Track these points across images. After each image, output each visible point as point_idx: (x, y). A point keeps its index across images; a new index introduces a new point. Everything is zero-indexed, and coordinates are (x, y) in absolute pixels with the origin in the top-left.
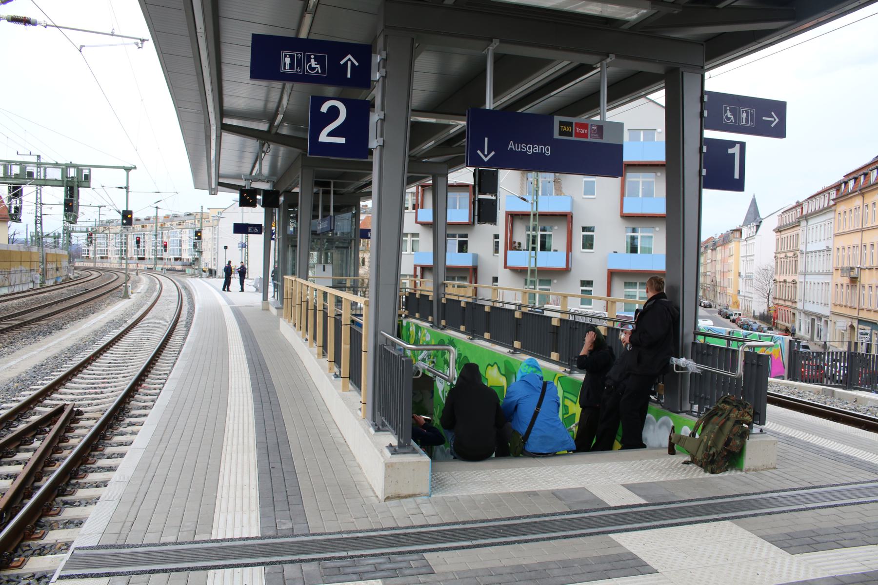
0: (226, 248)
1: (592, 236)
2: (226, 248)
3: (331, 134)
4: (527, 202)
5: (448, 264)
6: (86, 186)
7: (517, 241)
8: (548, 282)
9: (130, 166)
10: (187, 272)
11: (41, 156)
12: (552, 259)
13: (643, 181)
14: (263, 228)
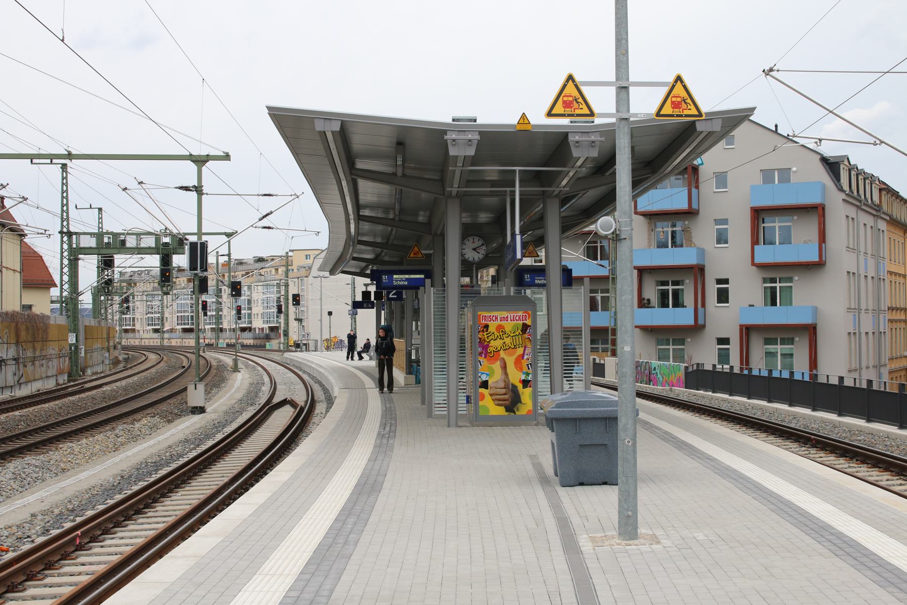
0: (330, 313)
2: (330, 313)
3: (392, 295)
4: (606, 268)
5: (564, 325)
6: (181, 253)
7: (646, 298)
8: (682, 342)
9: (231, 231)
10: (268, 347)
11: (103, 209)
12: (683, 317)
13: (779, 227)
14: (375, 304)
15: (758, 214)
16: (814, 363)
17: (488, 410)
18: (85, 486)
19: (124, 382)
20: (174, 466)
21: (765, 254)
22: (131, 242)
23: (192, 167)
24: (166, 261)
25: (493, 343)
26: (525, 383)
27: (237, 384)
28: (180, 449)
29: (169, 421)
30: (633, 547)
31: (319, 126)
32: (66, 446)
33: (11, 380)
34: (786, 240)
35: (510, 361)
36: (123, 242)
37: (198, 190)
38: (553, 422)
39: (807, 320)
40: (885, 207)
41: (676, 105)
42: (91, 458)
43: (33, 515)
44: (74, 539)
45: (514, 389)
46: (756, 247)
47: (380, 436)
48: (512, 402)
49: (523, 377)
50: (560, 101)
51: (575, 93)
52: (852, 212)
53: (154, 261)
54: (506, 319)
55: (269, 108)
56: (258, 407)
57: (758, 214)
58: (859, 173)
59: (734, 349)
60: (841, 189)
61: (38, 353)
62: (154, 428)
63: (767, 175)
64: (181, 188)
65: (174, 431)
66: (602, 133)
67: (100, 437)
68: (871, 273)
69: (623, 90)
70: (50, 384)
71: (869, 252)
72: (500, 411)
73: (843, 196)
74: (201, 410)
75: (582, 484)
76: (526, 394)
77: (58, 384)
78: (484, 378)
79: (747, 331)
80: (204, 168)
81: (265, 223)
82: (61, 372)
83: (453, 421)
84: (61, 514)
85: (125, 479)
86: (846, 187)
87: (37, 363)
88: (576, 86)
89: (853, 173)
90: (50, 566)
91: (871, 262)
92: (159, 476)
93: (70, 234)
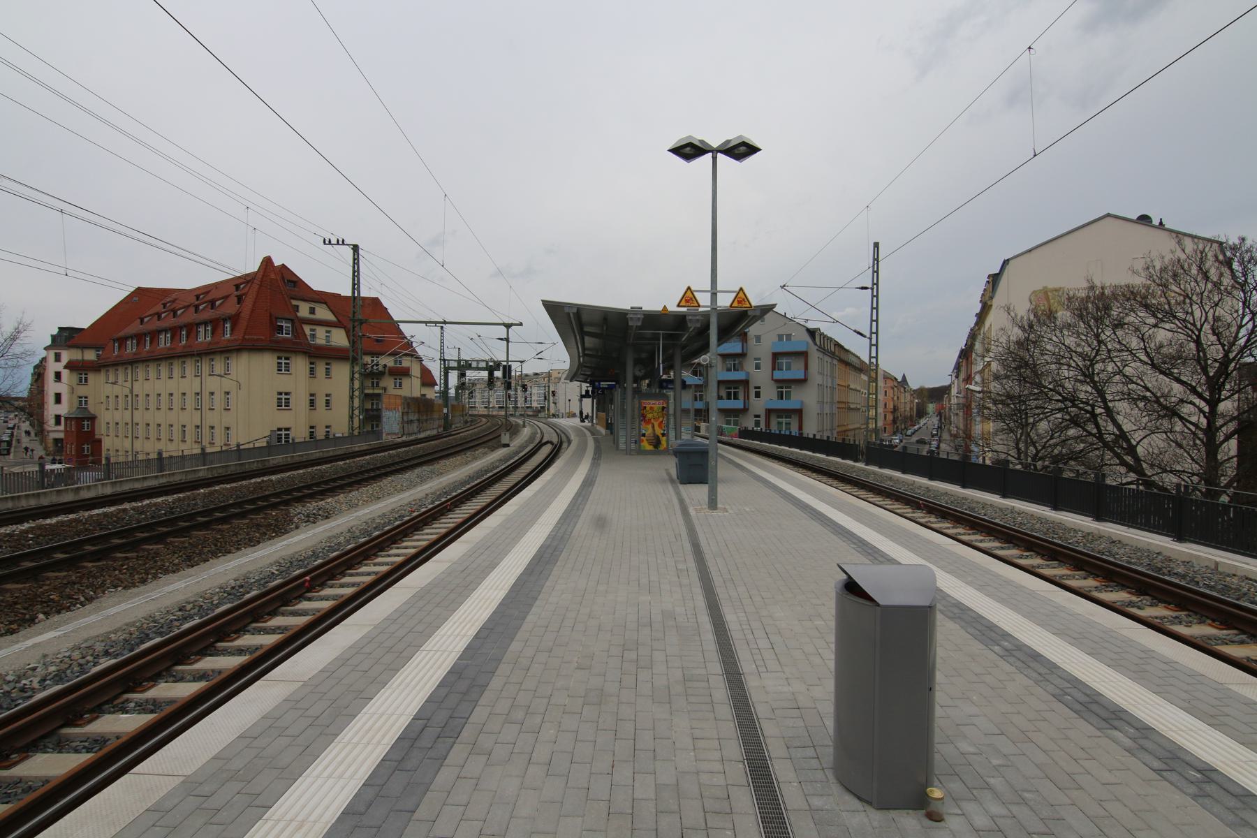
0: (570, 400)
1: (759, 391)
2: (570, 400)
5: (683, 407)
8: (737, 416)
12: (739, 404)
15: (776, 356)
16: (801, 428)
17: (644, 447)
18: (451, 481)
19: (470, 432)
20: (495, 472)
21: (779, 375)
22: (474, 365)
23: (505, 329)
24: (491, 374)
25: (648, 415)
26: (663, 435)
27: (525, 433)
28: (497, 464)
29: (492, 451)
30: (715, 513)
31: (567, 310)
32: (442, 462)
33: (416, 430)
34: (789, 368)
35: (656, 424)
36: (470, 365)
37: (507, 340)
38: (677, 453)
39: (798, 407)
40: (837, 353)
41: (739, 302)
42: (455, 467)
43: (427, 495)
44: (447, 506)
45: (658, 437)
46: (774, 372)
47: (594, 459)
48: (656, 443)
49: (662, 432)
50: (684, 300)
51: (692, 296)
52: (821, 355)
53: (485, 374)
54: (655, 404)
55: (542, 301)
56: (534, 444)
57: (776, 356)
58: (825, 336)
59: (762, 420)
60: (816, 344)
61: (429, 417)
62: (485, 454)
63: (780, 337)
64: (499, 339)
65: (494, 455)
66: (702, 316)
67: (459, 458)
68: (829, 385)
69: (714, 295)
70: (434, 432)
71: (829, 374)
72: (650, 448)
73: (817, 347)
74: (507, 445)
75: (690, 483)
76: (663, 440)
77: (438, 432)
78: (644, 432)
79: (769, 412)
80: (510, 329)
81: (539, 356)
82: (440, 426)
83: (628, 452)
84: (440, 494)
85: (471, 478)
86: (818, 343)
87: (428, 422)
88: (692, 292)
89: (822, 337)
90: (435, 519)
91: (830, 380)
92: (487, 477)
93: (444, 360)
